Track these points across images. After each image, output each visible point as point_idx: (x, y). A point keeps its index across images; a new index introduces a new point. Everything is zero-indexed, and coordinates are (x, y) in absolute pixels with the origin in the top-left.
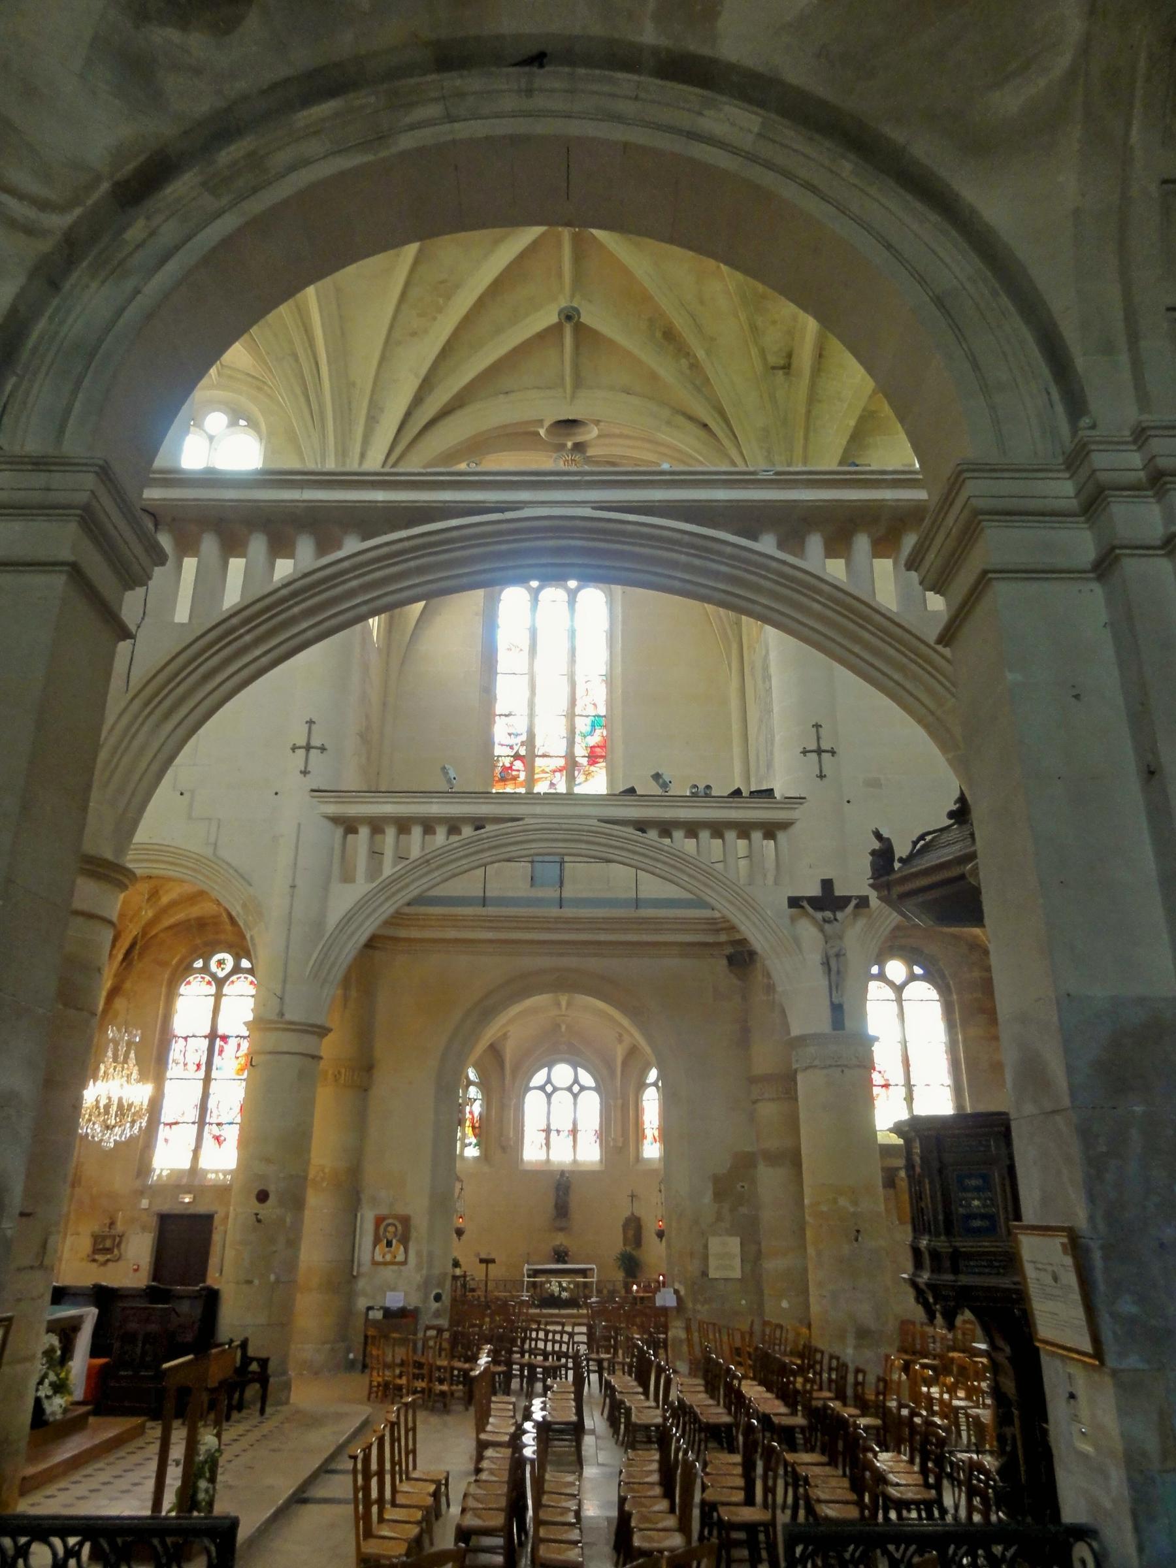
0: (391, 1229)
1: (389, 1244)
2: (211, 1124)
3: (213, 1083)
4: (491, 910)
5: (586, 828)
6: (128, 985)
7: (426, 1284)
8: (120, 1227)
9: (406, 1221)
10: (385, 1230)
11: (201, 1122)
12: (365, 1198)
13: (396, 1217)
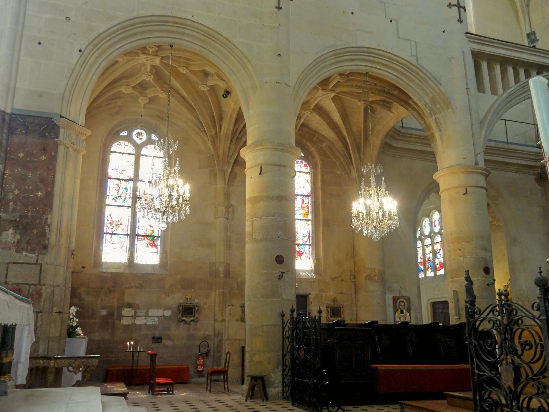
0: (402, 304)
1: (402, 312)
9: (408, 299)
10: (399, 305)
13: (403, 298)
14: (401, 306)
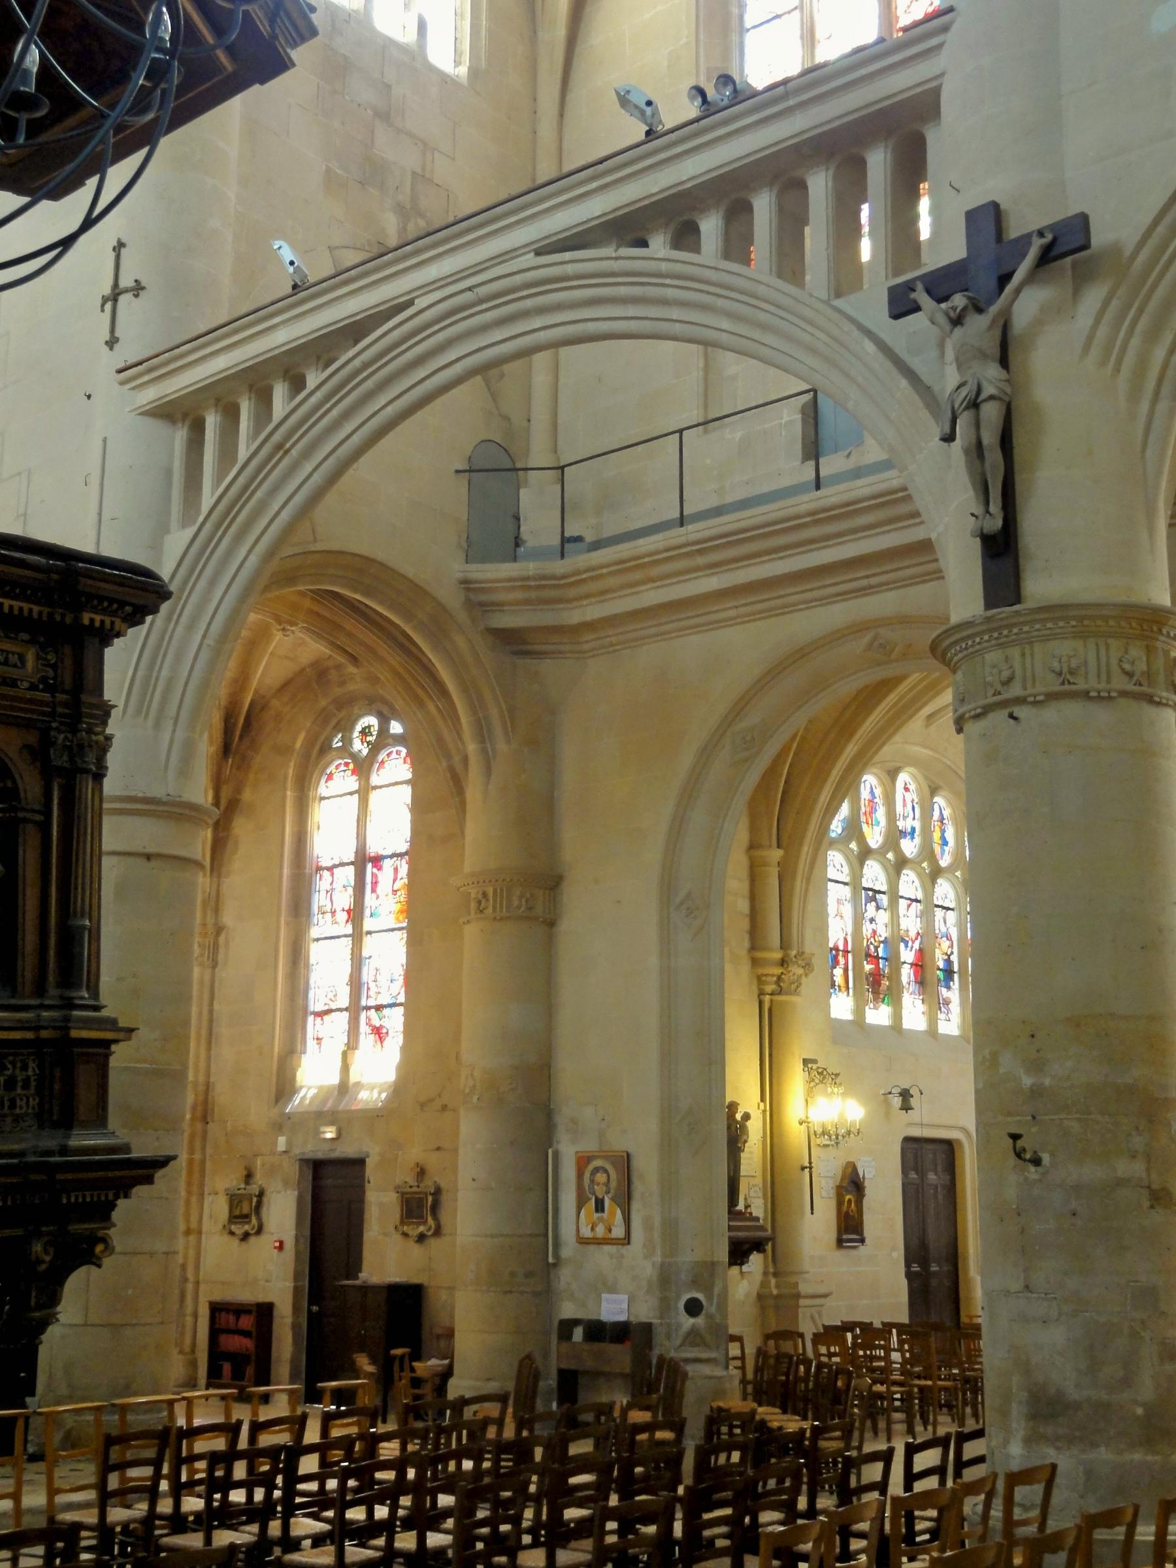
0: (601, 1177)
1: (600, 1207)
2: (368, 1008)
3: (368, 941)
4: (693, 531)
5: (518, 279)
6: (247, 795)
7: (665, 1279)
8: (259, 1179)
9: (625, 1164)
11: (355, 1009)
12: (561, 1121)
14: (598, 1184)
